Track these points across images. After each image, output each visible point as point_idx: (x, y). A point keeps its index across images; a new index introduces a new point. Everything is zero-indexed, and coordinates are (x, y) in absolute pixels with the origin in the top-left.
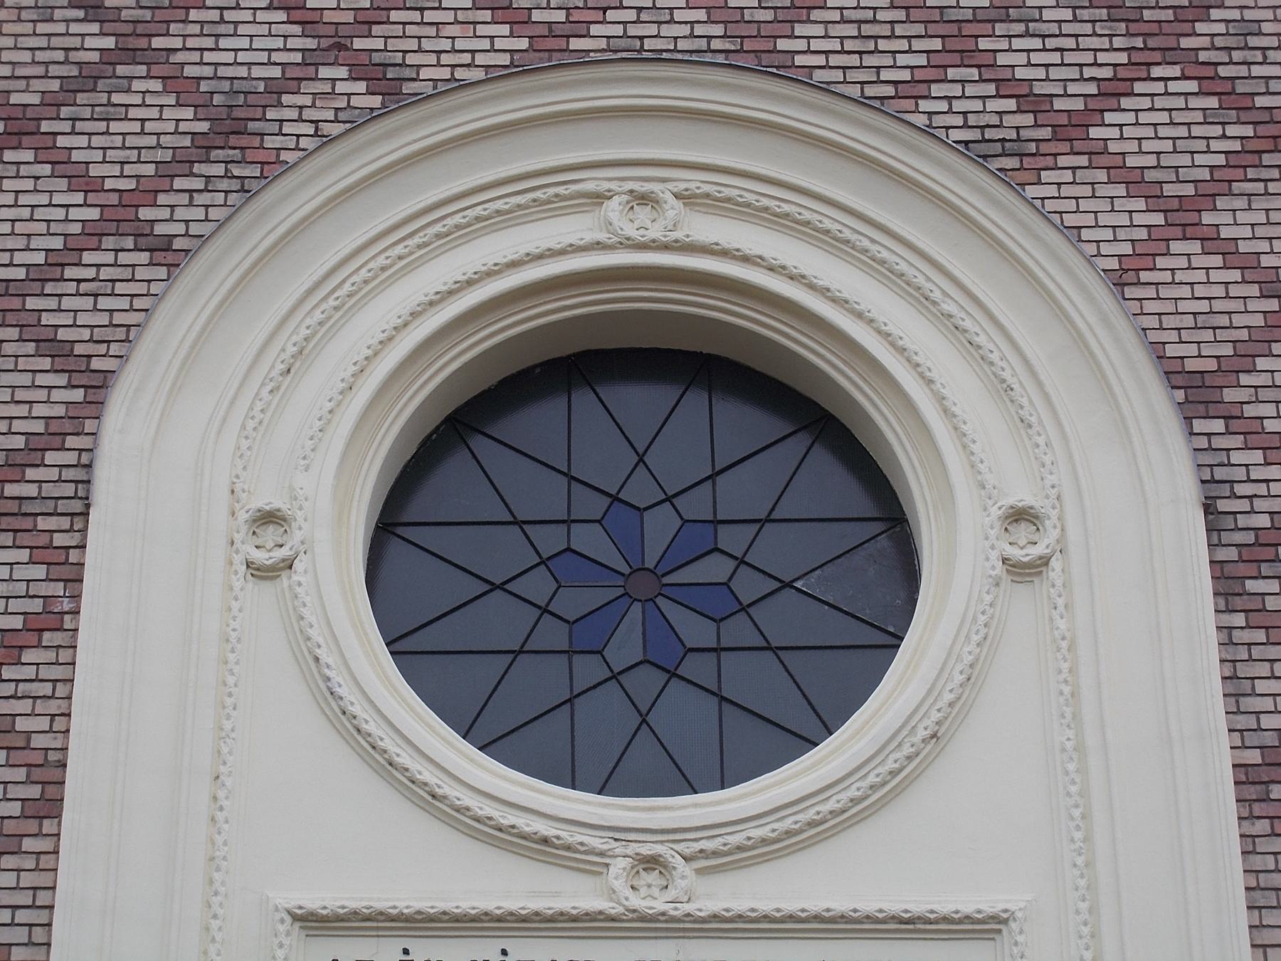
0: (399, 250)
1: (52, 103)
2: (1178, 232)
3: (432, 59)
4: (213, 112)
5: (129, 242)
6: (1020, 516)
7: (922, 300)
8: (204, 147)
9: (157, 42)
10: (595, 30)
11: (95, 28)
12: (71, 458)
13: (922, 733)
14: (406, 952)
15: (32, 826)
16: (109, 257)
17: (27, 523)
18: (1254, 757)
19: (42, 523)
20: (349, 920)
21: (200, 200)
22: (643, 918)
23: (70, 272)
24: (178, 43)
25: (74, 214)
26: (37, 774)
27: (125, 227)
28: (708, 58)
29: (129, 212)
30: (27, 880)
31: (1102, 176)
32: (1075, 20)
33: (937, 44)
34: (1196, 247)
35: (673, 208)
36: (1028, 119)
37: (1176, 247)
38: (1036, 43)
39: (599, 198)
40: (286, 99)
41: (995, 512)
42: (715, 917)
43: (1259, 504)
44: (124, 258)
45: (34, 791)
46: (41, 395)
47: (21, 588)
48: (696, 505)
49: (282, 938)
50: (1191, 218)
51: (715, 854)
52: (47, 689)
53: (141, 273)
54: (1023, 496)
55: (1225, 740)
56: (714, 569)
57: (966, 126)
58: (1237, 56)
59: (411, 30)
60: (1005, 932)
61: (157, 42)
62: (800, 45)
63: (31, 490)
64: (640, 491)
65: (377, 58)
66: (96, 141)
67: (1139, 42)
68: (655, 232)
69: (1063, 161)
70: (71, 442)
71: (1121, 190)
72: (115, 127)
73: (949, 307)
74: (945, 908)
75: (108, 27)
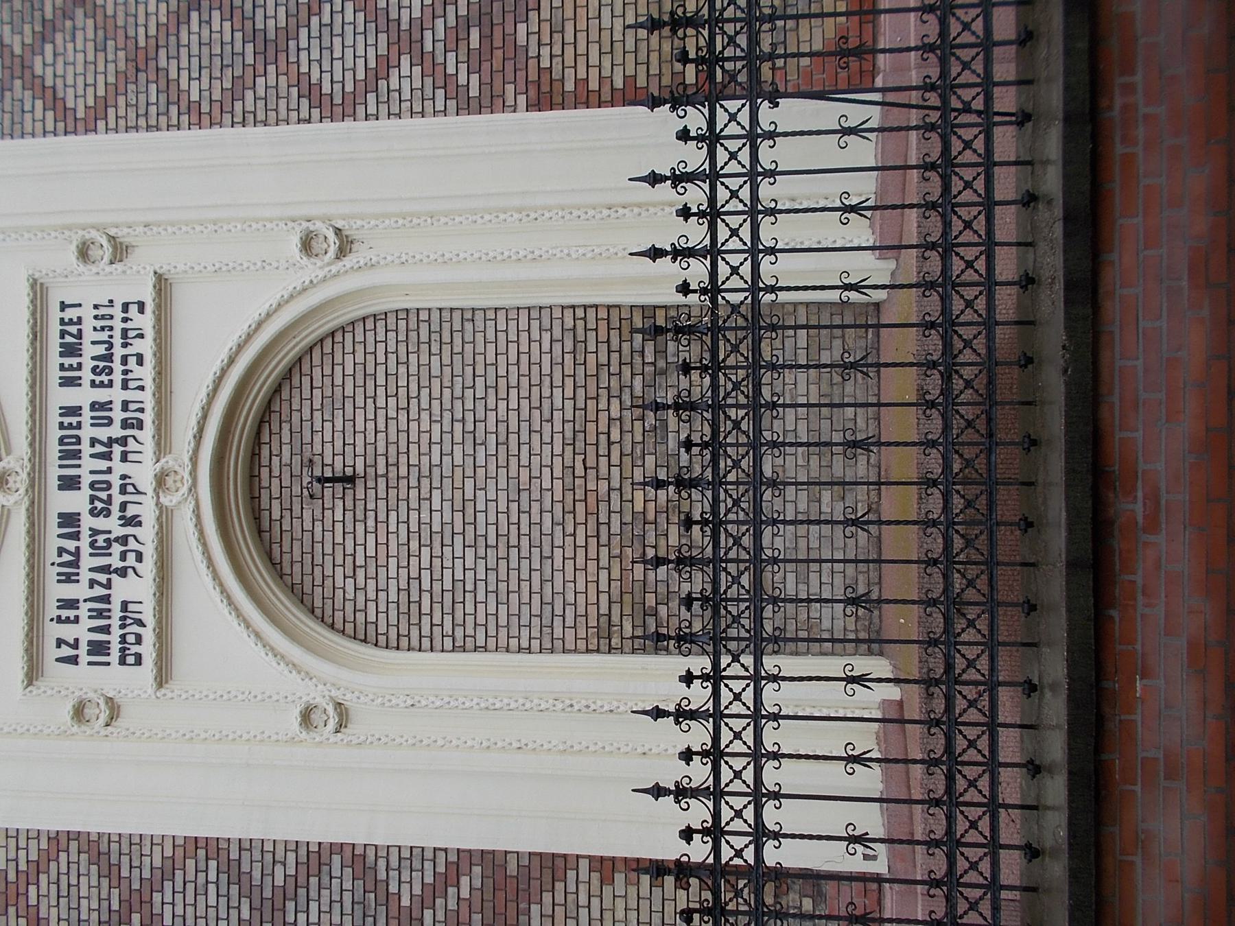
14: (52, 620)
20: (32, 653)
22: (32, 485)
42: (32, 445)
49: (40, 691)
60: (42, 281)
74: (26, 314)
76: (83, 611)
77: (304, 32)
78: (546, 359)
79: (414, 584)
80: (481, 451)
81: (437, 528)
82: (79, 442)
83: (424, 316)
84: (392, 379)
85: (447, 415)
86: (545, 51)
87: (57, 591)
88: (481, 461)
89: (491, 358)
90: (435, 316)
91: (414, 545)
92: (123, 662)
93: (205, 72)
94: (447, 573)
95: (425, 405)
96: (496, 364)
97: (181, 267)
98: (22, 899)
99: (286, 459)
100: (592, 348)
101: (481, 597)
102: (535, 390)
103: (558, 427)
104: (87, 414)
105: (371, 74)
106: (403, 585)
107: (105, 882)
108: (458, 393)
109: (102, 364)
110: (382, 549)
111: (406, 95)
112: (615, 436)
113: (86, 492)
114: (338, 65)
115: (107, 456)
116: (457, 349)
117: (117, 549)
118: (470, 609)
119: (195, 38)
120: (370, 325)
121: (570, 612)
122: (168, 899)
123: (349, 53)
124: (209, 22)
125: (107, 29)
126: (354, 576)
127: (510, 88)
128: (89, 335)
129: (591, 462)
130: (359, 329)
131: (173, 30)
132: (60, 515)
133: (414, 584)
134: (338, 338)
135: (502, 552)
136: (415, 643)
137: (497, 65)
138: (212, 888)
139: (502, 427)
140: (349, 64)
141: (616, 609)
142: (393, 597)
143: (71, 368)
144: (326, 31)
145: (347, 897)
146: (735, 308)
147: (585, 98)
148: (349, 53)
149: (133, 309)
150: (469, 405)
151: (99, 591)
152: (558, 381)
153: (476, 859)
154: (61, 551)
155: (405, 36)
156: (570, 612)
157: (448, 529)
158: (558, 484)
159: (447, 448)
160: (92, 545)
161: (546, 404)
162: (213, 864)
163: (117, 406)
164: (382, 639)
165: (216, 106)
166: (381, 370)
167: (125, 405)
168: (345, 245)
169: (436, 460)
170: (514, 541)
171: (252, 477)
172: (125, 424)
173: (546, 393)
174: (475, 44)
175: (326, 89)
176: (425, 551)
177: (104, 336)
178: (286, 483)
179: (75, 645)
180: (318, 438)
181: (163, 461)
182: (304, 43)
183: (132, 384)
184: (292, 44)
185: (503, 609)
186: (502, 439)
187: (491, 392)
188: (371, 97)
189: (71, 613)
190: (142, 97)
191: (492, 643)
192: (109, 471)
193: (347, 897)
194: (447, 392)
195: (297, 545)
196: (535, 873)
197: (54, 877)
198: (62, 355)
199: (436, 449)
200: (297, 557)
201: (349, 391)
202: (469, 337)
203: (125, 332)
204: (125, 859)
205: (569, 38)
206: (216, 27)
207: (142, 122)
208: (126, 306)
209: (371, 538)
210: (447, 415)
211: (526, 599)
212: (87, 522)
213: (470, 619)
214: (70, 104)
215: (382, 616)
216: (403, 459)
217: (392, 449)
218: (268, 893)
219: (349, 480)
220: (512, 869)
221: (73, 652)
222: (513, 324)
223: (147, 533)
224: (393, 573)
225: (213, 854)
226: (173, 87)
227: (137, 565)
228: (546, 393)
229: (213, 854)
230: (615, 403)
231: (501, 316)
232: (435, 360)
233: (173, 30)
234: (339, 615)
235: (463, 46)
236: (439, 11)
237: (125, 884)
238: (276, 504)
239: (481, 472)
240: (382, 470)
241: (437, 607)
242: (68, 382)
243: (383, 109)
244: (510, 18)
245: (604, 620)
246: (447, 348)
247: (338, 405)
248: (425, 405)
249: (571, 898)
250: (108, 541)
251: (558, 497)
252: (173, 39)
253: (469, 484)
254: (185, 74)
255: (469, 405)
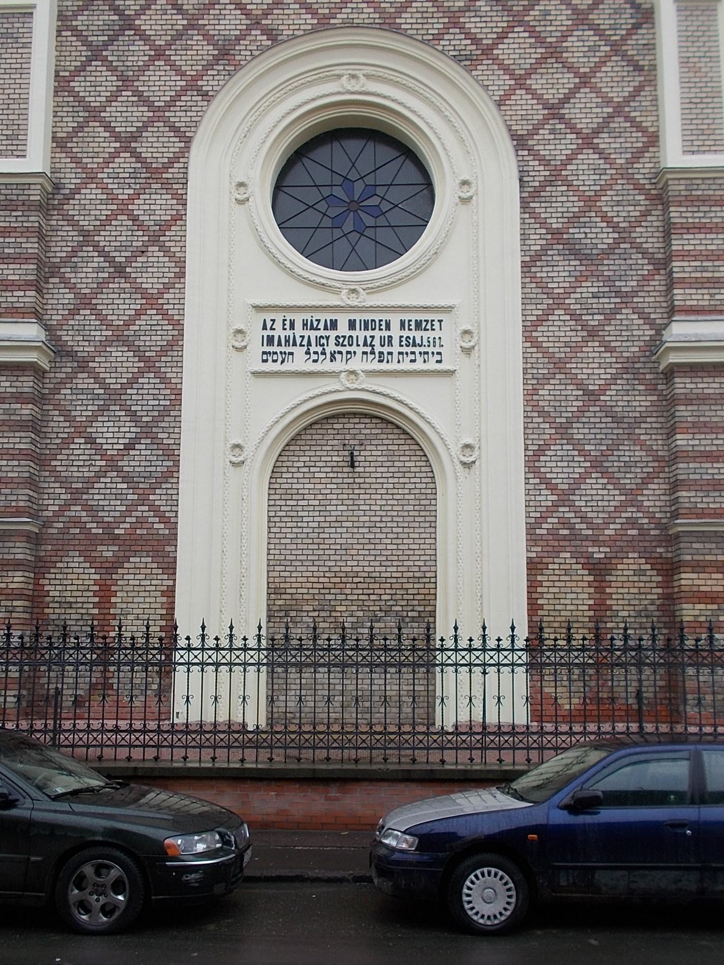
0: (278, 95)
1: (169, 45)
2: (518, 87)
3: (287, 27)
4: (219, 47)
5: (195, 93)
6: (465, 183)
7: (438, 111)
8: (217, 60)
9: (201, 22)
10: (338, 16)
11: (180, 17)
12: (181, 165)
13: (432, 252)
15: (178, 280)
16: (189, 98)
17: (170, 186)
18: (528, 259)
19: (175, 186)
21: (216, 78)
23: (178, 103)
24: (206, 22)
25: (178, 83)
26: (178, 264)
27: (194, 88)
28: (374, 26)
29: (194, 83)
30: (177, 296)
31: (496, 67)
32: (491, 11)
33: (446, 20)
34: (523, 92)
35: (363, 79)
36: (474, 47)
37: (518, 92)
38: (478, 19)
39: (339, 76)
40: (241, 42)
41: (458, 182)
42: (371, 307)
43: (536, 178)
44: (194, 98)
45: (177, 270)
46: (172, 145)
47: (169, 207)
48: (370, 180)
50: (522, 82)
51: (372, 288)
52: (179, 238)
53: (200, 104)
54: (466, 177)
55: (519, 254)
56: (374, 201)
57: (454, 50)
58: (542, 23)
59: (280, 17)
61: (201, 22)
62: (403, 21)
63: (170, 176)
64: (353, 176)
65: (270, 27)
66: (183, 58)
67: (511, 19)
68: (357, 88)
69: (484, 62)
70: (181, 160)
71: (502, 72)
72: (189, 52)
73: (447, 113)
74: (436, 304)
75: (185, 17)
76: (289, 333)
77: (571, 447)
78: (411, 563)
79: (301, 497)
80: (367, 530)
81: (328, 508)
82: (372, 329)
83: (433, 502)
84: (402, 486)
85: (384, 513)
86: (556, 566)
87: (299, 319)
88: (361, 530)
89: (411, 535)
90: (433, 508)
91: (320, 497)
92: (264, 353)
93: (552, 398)
94: (306, 514)
95: (389, 502)
96: (409, 538)
97: (458, 383)
98: (150, 307)
99: (364, 431)
100: (416, 586)
101: (294, 530)
102: (396, 558)
103: (377, 569)
104: (386, 334)
105: (549, 481)
106: (300, 491)
107: (159, 349)
108: (395, 519)
109: (411, 341)
110: (318, 481)
111: (538, 498)
112: (372, 597)
113: (348, 333)
114: (554, 464)
115: (365, 344)
116: (416, 519)
117: (319, 349)
118: (289, 525)
119: (569, 393)
120: (430, 475)
121: (287, 574)
122: (151, 381)
123: (560, 470)
124: (577, 400)
125: (575, 348)
126: (305, 466)
127: (539, 549)
128: (425, 334)
129: (360, 585)
130: (428, 469)
131: (574, 382)
132: (336, 320)
133: (301, 497)
134: (424, 458)
135: (316, 541)
136: (272, 497)
137: (551, 543)
138: (157, 402)
139: (378, 541)
140: (554, 470)
141: (289, 597)
142: (294, 486)
143: (410, 325)
144: (571, 458)
145: (153, 469)
146: (435, 657)
147: (533, 586)
148: (560, 470)
149: (438, 358)
150: (389, 525)
151: (298, 341)
152: (400, 569)
153: (172, 531)
154: (318, 321)
155: (566, 497)
156: (287, 574)
157: (328, 514)
158: (349, 569)
159: (367, 513)
160: (321, 337)
161: (389, 563)
162: (168, 403)
163: (390, 349)
164: (273, 481)
165: (535, 403)
166: (407, 480)
167: (390, 353)
168: (467, 465)
169: (362, 508)
170: (321, 547)
171: (355, 414)
172: (381, 353)
173: (395, 563)
174: (562, 532)
175: (542, 458)
176: (317, 503)
177: (425, 342)
178: (352, 431)
179: (271, 329)
180: (373, 448)
181: (362, 374)
182: (565, 447)
183: (401, 356)
184: (565, 441)
185: (289, 541)
186: (372, 541)
187: (395, 536)
188: (537, 481)
189: (287, 327)
190: (541, 366)
191: (272, 535)
192: (358, 345)
193: (153, 469)
194: (395, 513)
195: (320, 437)
196: (166, 560)
197: (161, 322)
198: (416, 321)
199: (367, 508)
200: (315, 437)
201: (396, 464)
202: (422, 525)
203: (427, 353)
204: (169, 359)
205: (562, 578)
206: (574, 403)
207: (529, 366)
208: (439, 353)
209: (324, 475)
210: (384, 513)
211: (293, 552)
212: (332, 334)
213: (283, 525)
214: (539, 329)
215: (285, 481)
216: (362, 491)
217: (367, 486)
218: (154, 430)
219: (353, 466)
220: (168, 549)
221: (268, 328)
222: (428, 547)
223: (326, 365)
224: (306, 486)
225: (173, 402)
226: (546, 381)
227: (311, 360)
228: (395, 563)
229: (173, 402)
230: (389, 597)
231: (432, 541)
232: (411, 508)
233: (574, 382)
234: (286, 459)
235: (561, 526)
236: (578, 515)
237: (158, 359)
238: (341, 426)
239: (356, 530)
240: (357, 480)
241: (290, 508)
242: (402, 324)
243: (532, 487)
244: (573, 549)
245: (283, 591)
246: (417, 513)
247: (390, 458)
248: (389, 502)
249: (155, 576)
250: (323, 345)
251: (343, 569)
252: (569, 382)
253: (350, 524)
254: (552, 387)
255: (389, 525)
